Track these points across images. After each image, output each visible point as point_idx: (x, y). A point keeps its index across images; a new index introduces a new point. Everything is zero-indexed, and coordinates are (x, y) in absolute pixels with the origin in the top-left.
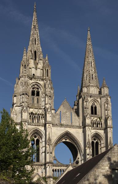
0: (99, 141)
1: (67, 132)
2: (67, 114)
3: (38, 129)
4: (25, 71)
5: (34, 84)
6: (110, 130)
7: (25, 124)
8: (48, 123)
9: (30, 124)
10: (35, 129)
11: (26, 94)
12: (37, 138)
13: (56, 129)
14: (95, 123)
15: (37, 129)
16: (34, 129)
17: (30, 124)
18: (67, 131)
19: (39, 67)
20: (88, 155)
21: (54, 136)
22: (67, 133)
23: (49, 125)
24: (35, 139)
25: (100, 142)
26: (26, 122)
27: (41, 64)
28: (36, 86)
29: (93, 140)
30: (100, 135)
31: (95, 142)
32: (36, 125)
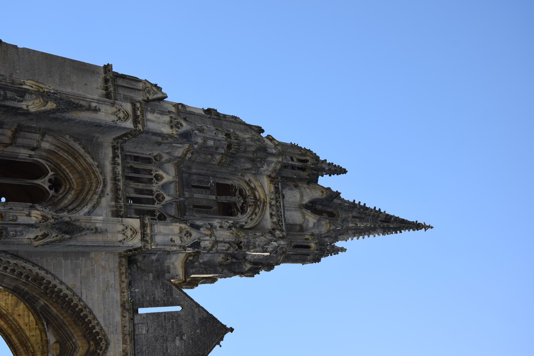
1: (103, 344)
2: (178, 343)
3: (99, 190)
4: (292, 160)
5: (259, 193)
7: (127, 116)
8: (143, 226)
9: (119, 152)
10: (101, 177)
11: (229, 147)
12: (52, 192)
13: (112, 282)
16: (98, 174)
17: (119, 152)
18: (108, 344)
19: (307, 217)
23: (135, 232)
24: (44, 183)
26: (136, 122)
27: (314, 224)
28: (250, 200)
32: (115, 179)
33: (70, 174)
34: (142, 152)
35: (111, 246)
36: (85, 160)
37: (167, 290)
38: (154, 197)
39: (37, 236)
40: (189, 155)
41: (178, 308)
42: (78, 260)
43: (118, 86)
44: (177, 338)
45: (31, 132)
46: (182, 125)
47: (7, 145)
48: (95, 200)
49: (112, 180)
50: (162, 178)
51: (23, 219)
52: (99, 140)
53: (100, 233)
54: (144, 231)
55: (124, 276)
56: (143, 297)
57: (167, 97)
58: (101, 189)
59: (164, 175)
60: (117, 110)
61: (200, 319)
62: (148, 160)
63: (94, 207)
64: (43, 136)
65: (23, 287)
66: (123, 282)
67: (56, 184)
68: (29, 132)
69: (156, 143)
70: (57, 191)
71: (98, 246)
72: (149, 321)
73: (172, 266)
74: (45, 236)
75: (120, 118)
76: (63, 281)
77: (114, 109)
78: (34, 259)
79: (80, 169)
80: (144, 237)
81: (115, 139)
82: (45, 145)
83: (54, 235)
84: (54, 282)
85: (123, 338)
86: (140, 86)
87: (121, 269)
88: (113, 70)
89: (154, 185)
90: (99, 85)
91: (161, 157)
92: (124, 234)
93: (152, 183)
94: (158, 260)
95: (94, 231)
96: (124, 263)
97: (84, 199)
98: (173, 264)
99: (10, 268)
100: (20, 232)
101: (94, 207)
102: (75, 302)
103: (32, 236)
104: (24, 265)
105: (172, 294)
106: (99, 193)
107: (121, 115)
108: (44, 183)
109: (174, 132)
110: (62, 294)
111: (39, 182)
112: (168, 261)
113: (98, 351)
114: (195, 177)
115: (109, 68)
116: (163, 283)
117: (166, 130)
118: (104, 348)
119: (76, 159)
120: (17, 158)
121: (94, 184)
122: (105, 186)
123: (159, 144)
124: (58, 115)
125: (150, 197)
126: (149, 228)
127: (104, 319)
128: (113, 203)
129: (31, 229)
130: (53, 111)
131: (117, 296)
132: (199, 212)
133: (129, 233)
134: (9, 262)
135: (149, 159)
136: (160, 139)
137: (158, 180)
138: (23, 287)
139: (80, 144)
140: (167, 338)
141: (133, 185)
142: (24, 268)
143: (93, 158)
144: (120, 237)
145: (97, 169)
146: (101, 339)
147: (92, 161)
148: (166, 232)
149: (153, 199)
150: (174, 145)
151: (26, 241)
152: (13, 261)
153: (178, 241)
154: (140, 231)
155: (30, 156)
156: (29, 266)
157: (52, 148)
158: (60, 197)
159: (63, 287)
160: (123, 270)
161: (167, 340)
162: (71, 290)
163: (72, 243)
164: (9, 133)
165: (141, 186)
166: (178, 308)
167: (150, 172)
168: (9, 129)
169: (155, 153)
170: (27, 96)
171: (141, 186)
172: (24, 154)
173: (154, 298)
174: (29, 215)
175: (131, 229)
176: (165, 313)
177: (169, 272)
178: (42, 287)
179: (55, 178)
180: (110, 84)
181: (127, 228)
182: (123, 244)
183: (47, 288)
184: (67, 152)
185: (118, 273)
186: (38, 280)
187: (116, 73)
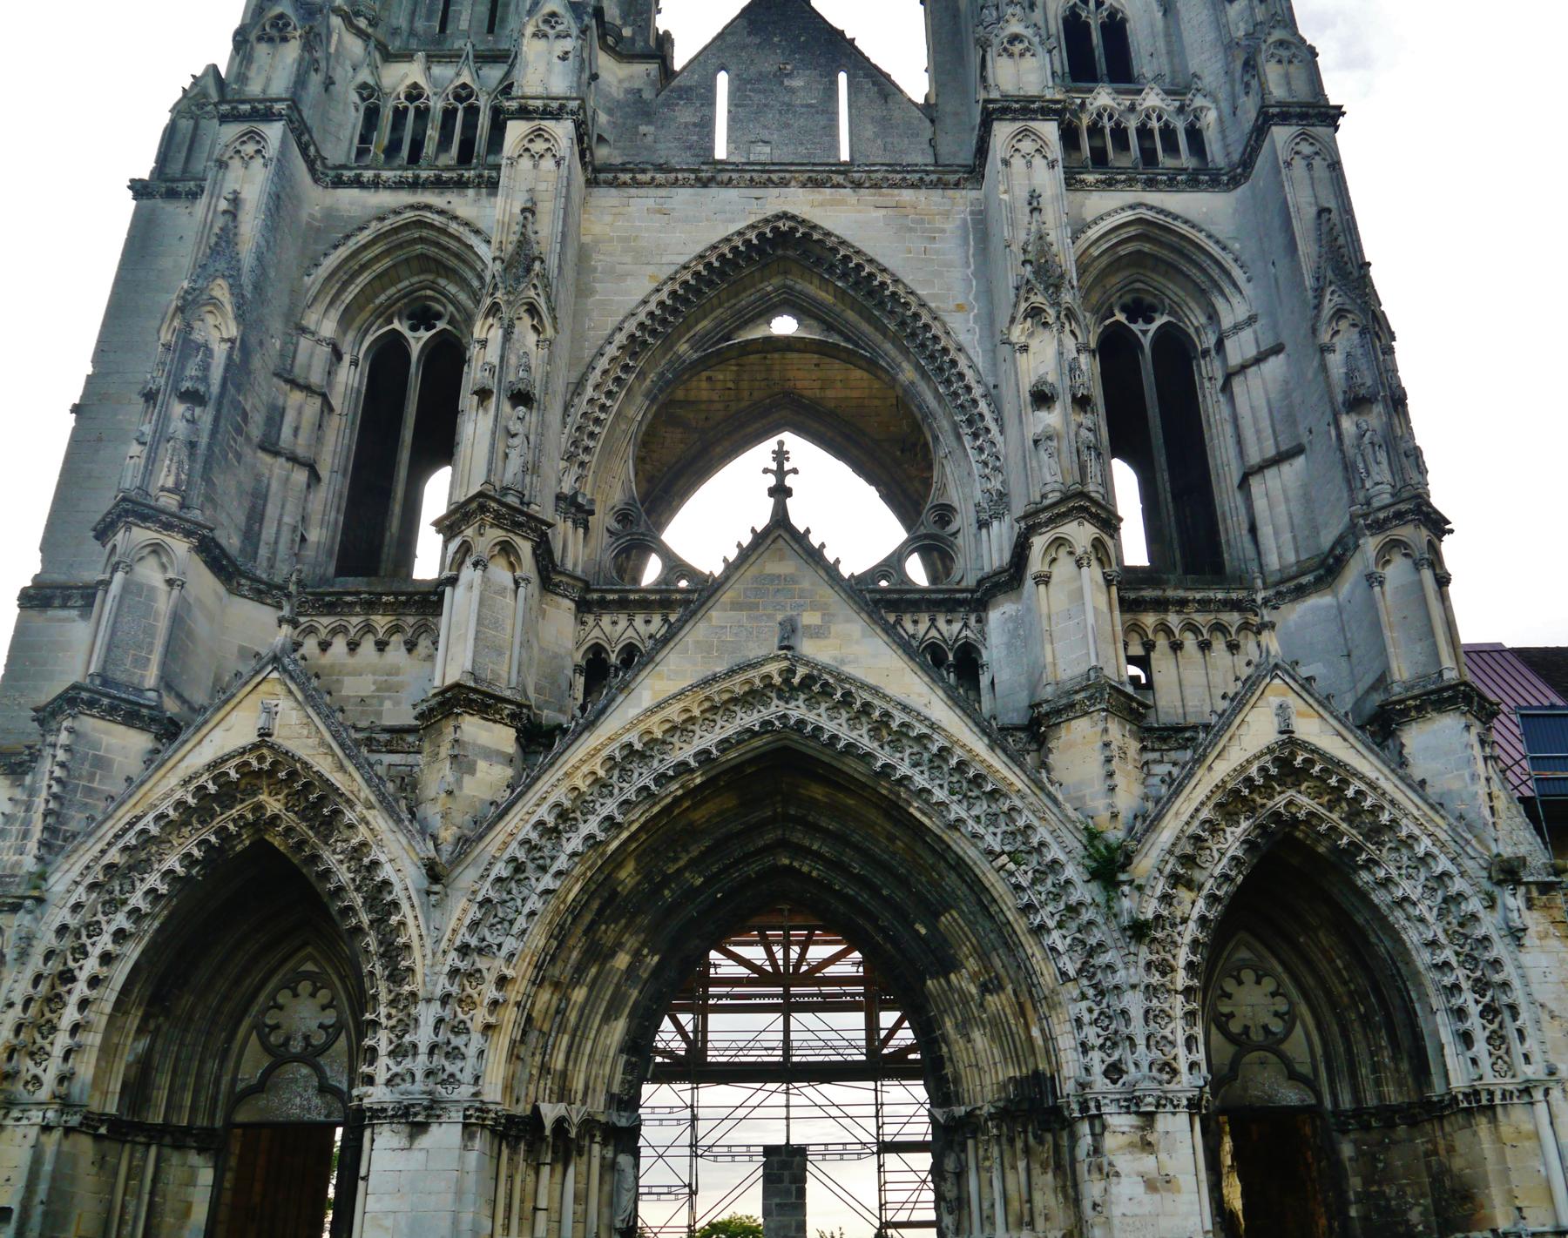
0: (1195, 318)
1: (783, 226)
2: (797, 83)
3: (438, 220)
6: (1306, 149)
8: (524, 113)
12: (441, 325)
13: (650, 203)
14: (1120, 134)
15: (430, 217)
17: (347, 174)
18: (785, 216)
20: (1042, 398)
21: (622, 277)
22: (782, 238)
23: (538, 133)
24: (417, 341)
25: (1213, 317)
26: (268, 116)
29: (1120, 317)
30: (1200, 238)
31: (1146, 332)
32: (415, 185)
33: (400, 286)
34: (350, 126)
35: (569, 185)
36: (365, 247)
37: (680, 98)
38: (460, 107)
39: (533, 327)
40: (362, 23)
41: (722, 79)
42: (595, 269)
43: (185, 170)
44: (786, 82)
45: (295, 352)
46: (281, 16)
47: (327, 406)
48: (461, 229)
49: (415, 193)
50: (415, 86)
51: (492, 354)
52: (318, 215)
53: (535, 204)
54: (536, 111)
55: (639, 176)
56: (690, 148)
57: (215, 67)
58: (435, 217)
59: (409, 82)
60: (237, 157)
61: (749, 34)
62: (372, 116)
63: (477, 232)
64: (304, 330)
65: (648, 382)
66: (653, 179)
67: (422, 317)
68: (294, 358)
69: (327, 90)
70: (439, 316)
71: (565, 209)
72: (745, 139)
73: (626, 85)
74: (532, 310)
75: (258, 151)
76: (640, 298)
77: (236, 163)
78: (588, 354)
79: (386, 263)
80: (551, 113)
81: (316, 181)
82: (328, 328)
83: (532, 293)
84: (642, 317)
85: (776, 185)
86: (185, 125)
87: (625, 184)
88: (146, 176)
89: (431, 104)
90: (182, 210)
91: (364, 86)
92: (542, 156)
93: (427, 109)
94: (610, 112)
95: (529, 215)
96: (610, 176)
97: (457, 256)
98: (620, 81)
99: (603, 400)
100: (519, 358)
101: (477, 232)
102: (688, 277)
103: (532, 338)
104: (598, 372)
105: (690, 88)
106: (443, 219)
107: (250, 148)
108: (417, 341)
109: (298, 33)
110: (669, 302)
111: (415, 349)
112: (614, 91)
113: (798, 235)
114: (420, 25)
115: (138, 186)
116: (663, 105)
117: (291, 52)
118: (792, 224)
119: (364, 268)
120: (359, 391)
121: (425, 233)
122: (428, 207)
123: (329, 83)
124: (246, 280)
125: (460, 115)
126: (530, 102)
127: (733, 221)
128: (471, 192)
129: (515, 336)
130: (236, 289)
131: (683, 194)
132: (503, 20)
133: (539, 146)
134: (591, 401)
135: (368, 109)
136: (316, 79)
137: (420, 96)
138: (648, 382)
139: (326, 255)
140: (784, 103)
141: (429, 148)
142: (605, 372)
143: (361, 229)
144: (548, 164)
145: (387, 222)
146: (775, 230)
147: (366, 232)
148: (542, 68)
149: (466, 110)
150: (332, 50)
151: (543, 352)
152: (589, 392)
153: (568, 44)
154: (537, 122)
155: (355, 363)
156: (603, 363)
157: (335, 315)
158: (451, 308)
159: (654, 299)
160: (626, 177)
161: (789, 105)
162: (665, 283)
163: (553, 262)
164: (297, 397)
165: (433, 133)
166: (722, 79)
167: (400, 114)
168: (286, 395)
169: (355, 98)
170: (197, 336)
171: (433, 133)
172: (349, 379)
173: (695, 125)
174: (484, 343)
175: (531, 141)
176: (730, 105)
177: (640, 91)
178: (650, 340)
179: (409, 318)
180: (180, 187)
181: (527, 150)
182: (563, 158)
183: (653, 333)
184: (345, 285)
185: (633, 191)
186: (634, 346)
187: (152, 173)
